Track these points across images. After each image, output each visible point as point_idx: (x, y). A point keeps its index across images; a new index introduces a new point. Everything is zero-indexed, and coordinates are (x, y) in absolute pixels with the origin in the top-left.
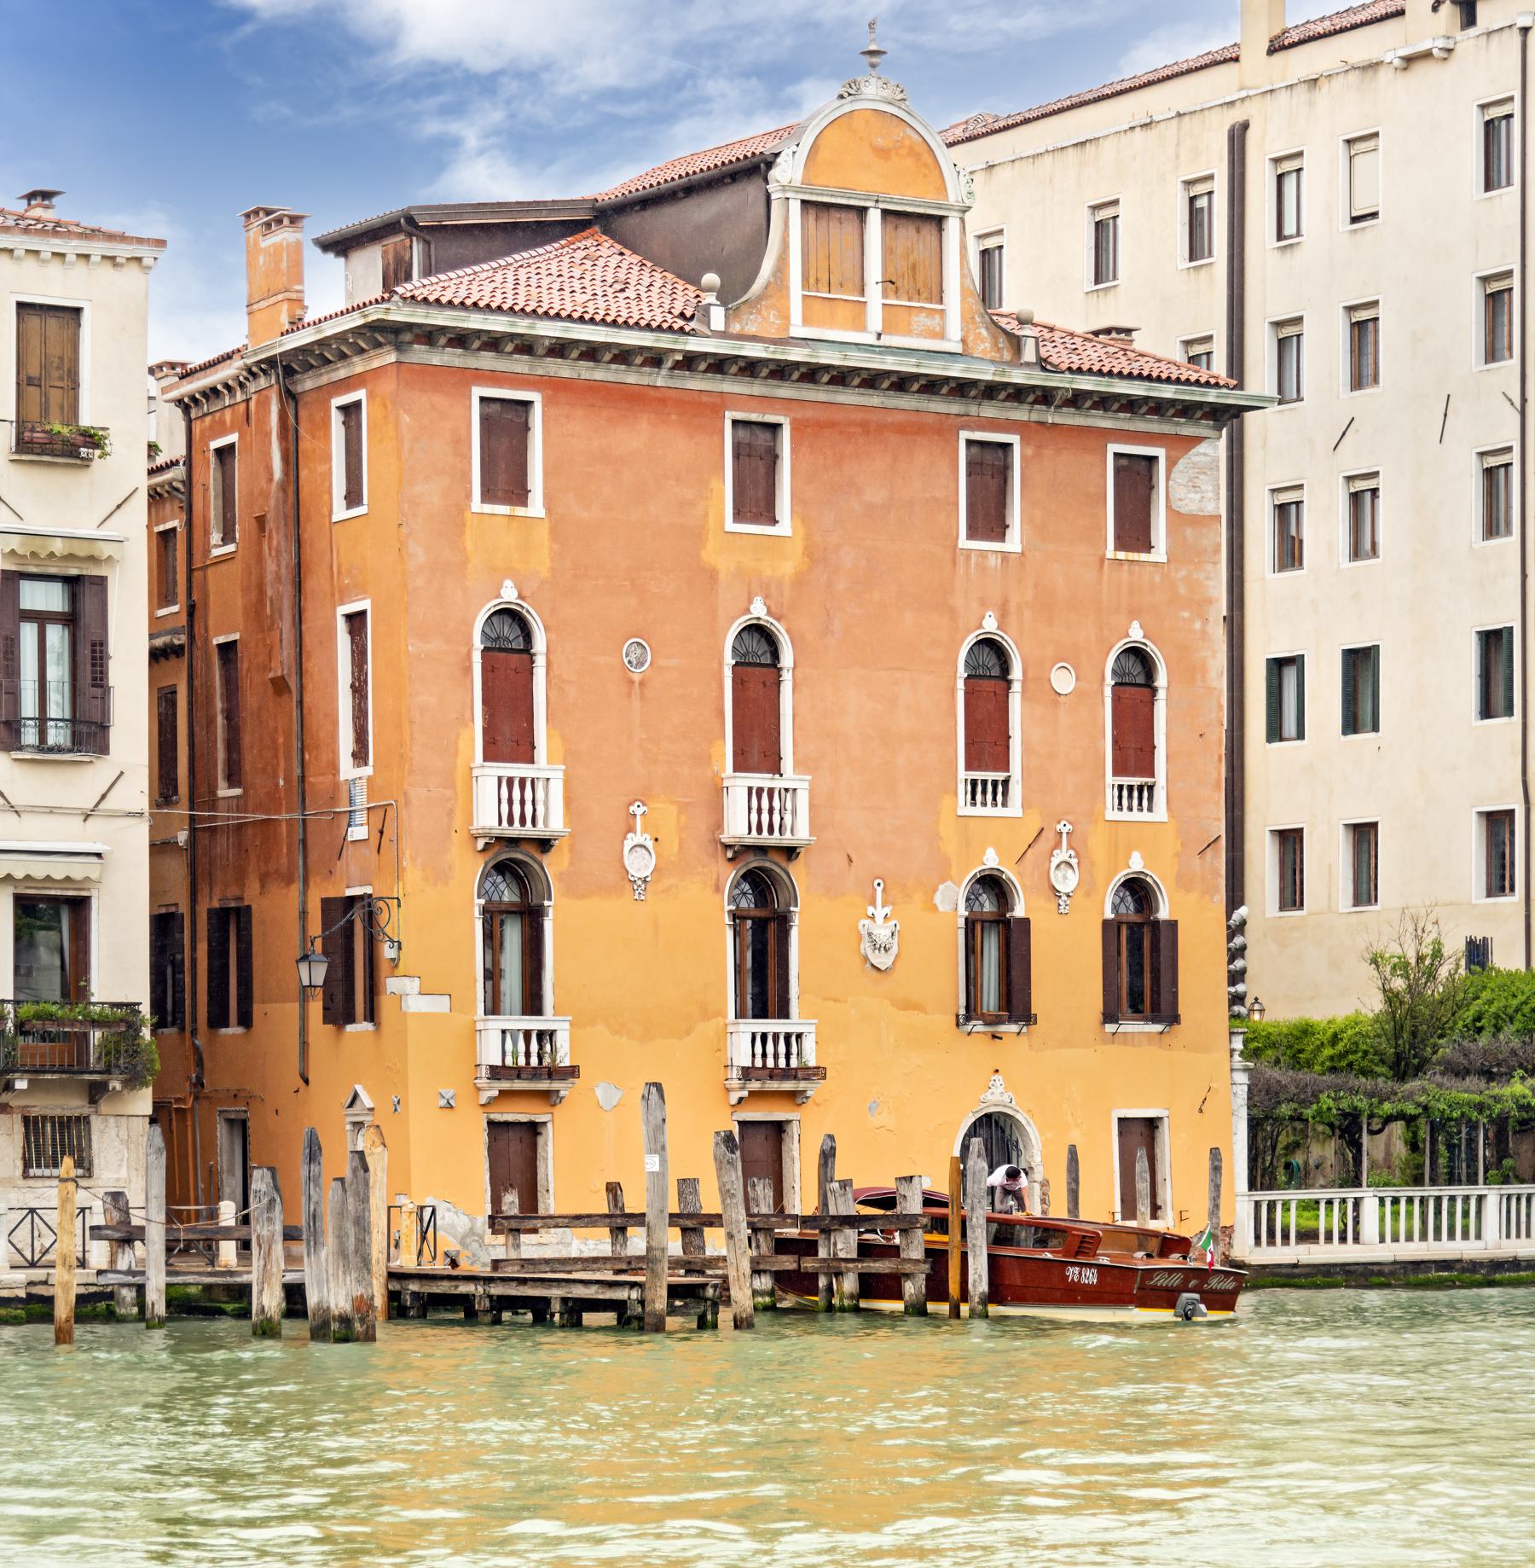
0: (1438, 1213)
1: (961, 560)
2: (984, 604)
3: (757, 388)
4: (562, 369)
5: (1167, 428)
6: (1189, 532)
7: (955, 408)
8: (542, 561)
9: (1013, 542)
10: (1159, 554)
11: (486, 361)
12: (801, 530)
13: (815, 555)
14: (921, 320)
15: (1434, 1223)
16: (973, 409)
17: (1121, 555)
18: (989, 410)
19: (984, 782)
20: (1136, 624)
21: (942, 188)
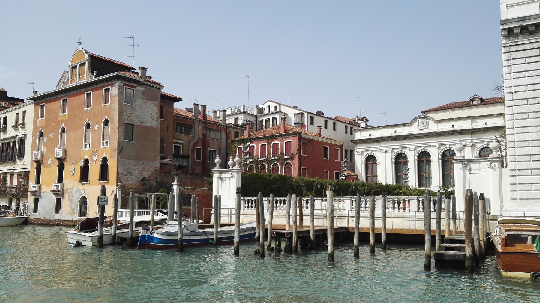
11: (41, 101)
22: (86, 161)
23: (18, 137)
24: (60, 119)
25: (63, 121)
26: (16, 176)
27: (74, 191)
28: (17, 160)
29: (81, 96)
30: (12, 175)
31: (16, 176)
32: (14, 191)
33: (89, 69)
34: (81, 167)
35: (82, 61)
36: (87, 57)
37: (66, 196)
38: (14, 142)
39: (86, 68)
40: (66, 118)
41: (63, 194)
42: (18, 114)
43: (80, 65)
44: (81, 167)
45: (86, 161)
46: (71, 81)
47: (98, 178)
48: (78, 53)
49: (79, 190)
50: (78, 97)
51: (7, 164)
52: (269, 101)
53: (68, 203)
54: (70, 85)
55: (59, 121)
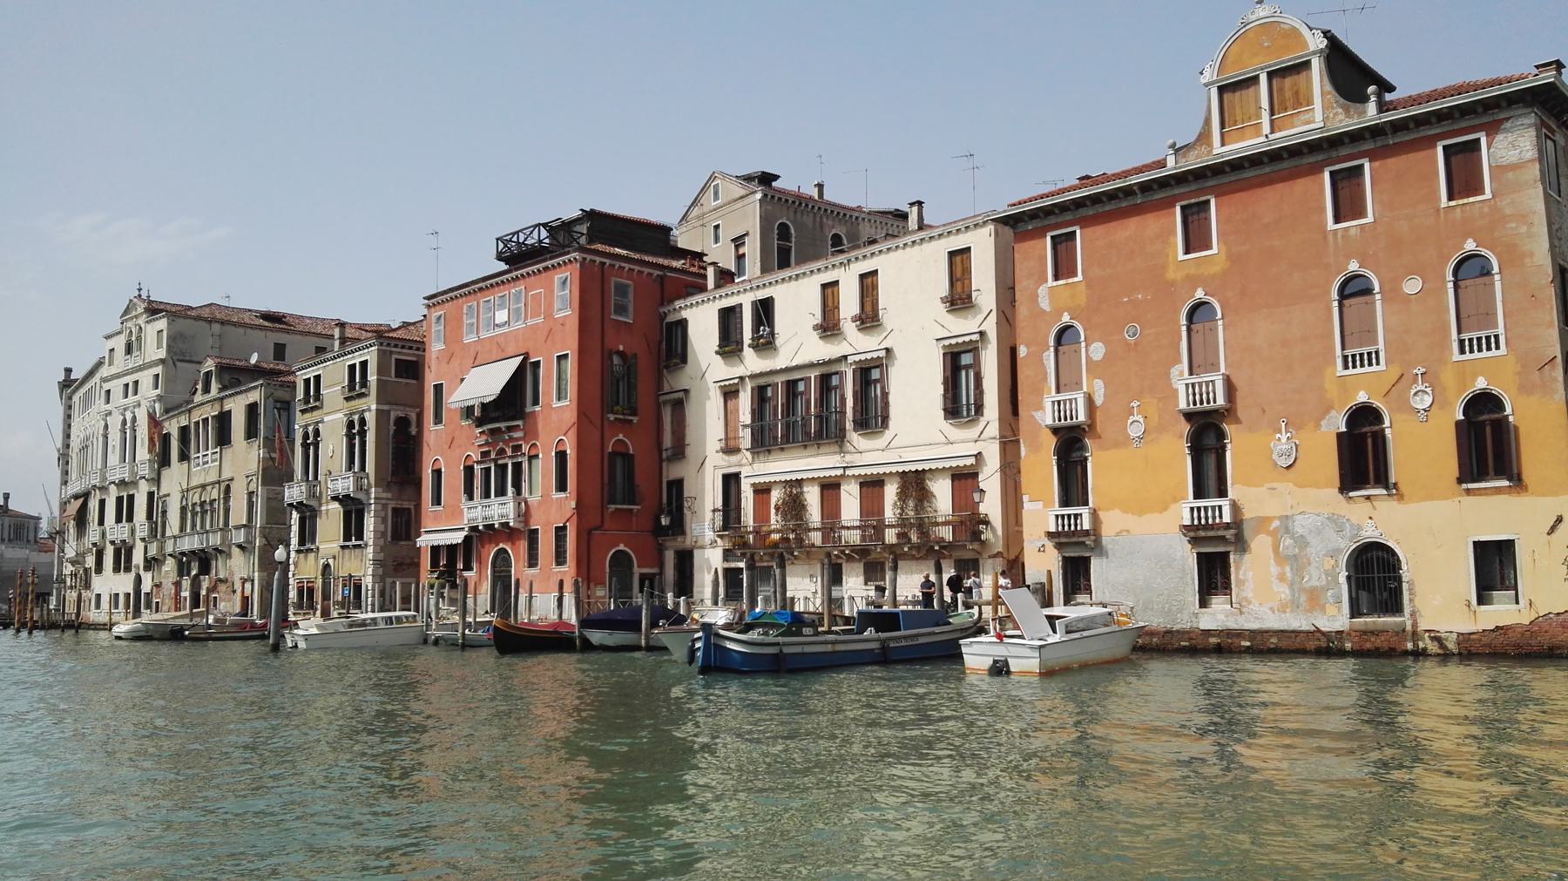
1: (1331, 238)
2: (1349, 257)
3: (1193, 187)
5: (1484, 120)
6: (1510, 175)
7: (1321, 157)
8: (1082, 300)
9: (1370, 219)
10: (1488, 194)
11: (1052, 220)
12: (1224, 249)
13: (1234, 259)
14: (1303, 117)
16: (1334, 154)
17: (1453, 203)
18: (1344, 152)
19: (1361, 355)
20: (1470, 241)
21: (1305, 45)
22: (1364, 416)
23: (850, 359)
24: (1171, 274)
26: (891, 491)
27: (1300, 525)
28: (854, 438)
29: (1301, 185)
30: (830, 488)
31: (891, 491)
32: (854, 537)
33: (1328, 87)
34: (1340, 435)
35: (1289, 58)
36: (1318, 42)
37: (1260, 544)
38: (826, 383)
41: (1241, 543)
42: (829, 288)
43: (1271, 75)
44: (1340, 435)
46: (1222, 135)
47: (1457, 474)
48: (1245, 37)
49: (1336, 522)
50: (1280, 186)
51: (783, 455)
53: (1274, 569)
54: (1221, 150)
55: (1173, 283)
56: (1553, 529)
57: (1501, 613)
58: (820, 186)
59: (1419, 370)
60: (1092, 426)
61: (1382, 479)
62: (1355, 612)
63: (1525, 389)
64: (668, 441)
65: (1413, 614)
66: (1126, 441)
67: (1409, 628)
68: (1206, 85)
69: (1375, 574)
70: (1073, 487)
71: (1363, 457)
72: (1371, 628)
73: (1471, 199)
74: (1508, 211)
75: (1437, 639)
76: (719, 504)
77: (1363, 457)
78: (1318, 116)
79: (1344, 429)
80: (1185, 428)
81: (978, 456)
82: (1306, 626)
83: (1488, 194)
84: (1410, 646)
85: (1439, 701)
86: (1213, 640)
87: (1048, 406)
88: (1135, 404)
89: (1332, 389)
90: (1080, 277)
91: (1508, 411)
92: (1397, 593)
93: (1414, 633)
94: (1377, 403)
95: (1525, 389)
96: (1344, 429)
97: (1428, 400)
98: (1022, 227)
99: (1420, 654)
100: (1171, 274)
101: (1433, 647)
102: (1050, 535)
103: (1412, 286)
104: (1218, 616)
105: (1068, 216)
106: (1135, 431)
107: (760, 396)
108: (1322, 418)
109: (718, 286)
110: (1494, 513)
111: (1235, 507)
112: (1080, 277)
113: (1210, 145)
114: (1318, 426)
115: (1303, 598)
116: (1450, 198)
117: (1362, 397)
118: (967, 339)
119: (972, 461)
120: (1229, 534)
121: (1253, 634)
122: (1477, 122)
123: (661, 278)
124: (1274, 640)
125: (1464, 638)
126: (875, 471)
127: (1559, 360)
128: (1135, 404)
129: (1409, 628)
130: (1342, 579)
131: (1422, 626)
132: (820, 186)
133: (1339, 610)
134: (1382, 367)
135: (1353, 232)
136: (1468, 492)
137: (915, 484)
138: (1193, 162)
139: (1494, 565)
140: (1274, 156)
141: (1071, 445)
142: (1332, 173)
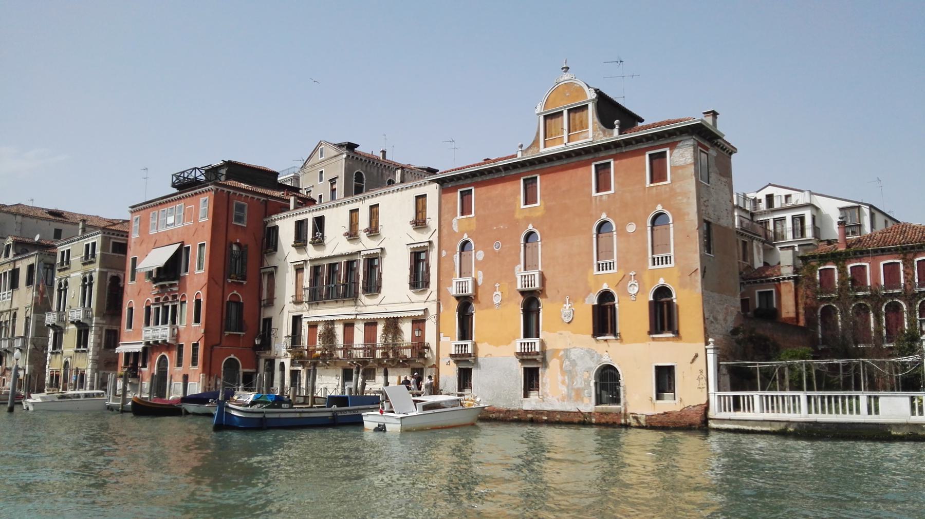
0: (823, 403)
3: (530, 169)
4: (479, 179)
5: (669, 141)
6: (680, 171)
7: (591, 157)
8: (474, 227)
10: (669, 181)
11: (461, 182)
13: (548, 209)
14: (584, 135)
15: (829, 404)
16: (597, 155)
18: (602, 154)
21: (586, 96)
22: (606, 296)
23: (362, 253)
24: (518, 216)
25: (528, 220)
26: (380, 328)
27: (574, 354)
28: (363, 298)
29: (580, 171)
30: (349, 325)
31: (380, 328)
32: (360, 354)
33: (596, 120)
34: (594, 306)
35: (578, 103)
36: (592, 95)
37: (554, 363)
38: (350, 266)
39: (591, 113)
40: (539, 214)
41: (544, 362)
42: (354, 212)
43: (569, 111)
44: (594, 306)
45: (606, 296)
46: (545, 142)
47: (648, 329)
49: (590, 353)
50: (571, 171)
52: (770, 185)
53: (560, 378)
54: (544, 151)
55: (518, 221)
56: (693, 360)
57: (668, 405)
58: (384, 152)
59: (633, 273)
60: (476, 296)
61: (614, 332)
62: (599, 401)
63: (683, 285)
64: (265, 296)
65: (625, 404)
66: (491, 305)
67: (623, 411)
68: (538, 114)
69: (608, 381)
70: (465, 332)
71: (604, 320)
72: (605, 411)
73: (661, 183)
74: (678, 190)
75: (636, 418)
76: (290, 333)
77: (604, 320)
78: (591, 135)
79: (596, 303)
80: (521, 299)
81: (426, 310)
82: (574, 409)
83: (669, 181)
84: (623, 421)
85: (639, 449)
86: (529, 416)
87: (454, 284)
88: (497, 285)
89: (591, 282)
90: (473, 215)
91: (674, 297)
92: (618, 394)
93: (625, 414)
94: (612, 290)
95: (683, 285)
96: (596, 303)
97: (636, 289)
98: (446, 185)
99: (627, 426)
100: (518, 216)
101: (634, 423)
102: (451, 355)
103: (631, 228)
104: (533, 403)
105: (468, 181)
106: (497, 300)
107: (316, 271)
108: (586, 296)
109: (296, 208)
110: (665, 351)
111: (543, 344)
112: (473, 215)
113: (538, 147)
114: (584, 301)
115: (573, 394)
116: (652, 182)
117: (605, 287)
118: (422, 245)
119: (422, 313)
120: (538, 358)
121: (549, 413)
122: (665, 142)
123: (266, 202)
124: (558, 416)
125: (649, 418)
126: (372, 317)
127: (699, 271)
128: (497, 285)
129: (623, 411)
130: (593, 382)
131: (629, 411)
132: (384, 152)
133: (590, 400)
134: (615, 271)
135: (604, 198)
136: (654, 339)
137: (393, 325)
138: (529, 156)
139: (665, 378)
140: (568, 155)
141: (465, 305)
142: (596, 166)
